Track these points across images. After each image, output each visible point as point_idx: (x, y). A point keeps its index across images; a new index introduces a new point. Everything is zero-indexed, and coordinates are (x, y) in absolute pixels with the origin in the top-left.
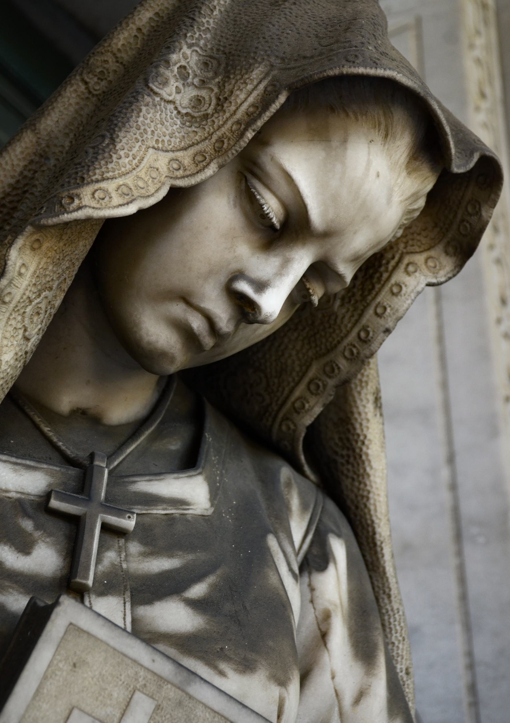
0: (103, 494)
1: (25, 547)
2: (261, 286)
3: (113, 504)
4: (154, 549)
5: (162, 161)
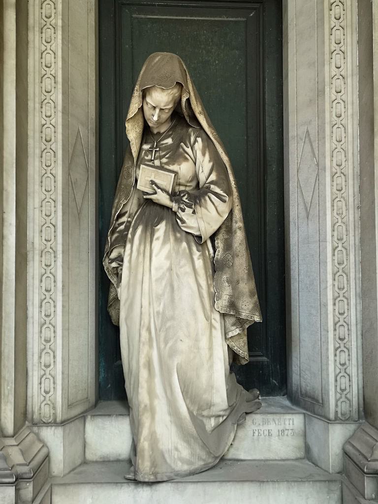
0: (155, 146)
1: (147, 156)
2: (153, 116)
3: (157, 147)
4: (163, 152)
5: (137, 105)
